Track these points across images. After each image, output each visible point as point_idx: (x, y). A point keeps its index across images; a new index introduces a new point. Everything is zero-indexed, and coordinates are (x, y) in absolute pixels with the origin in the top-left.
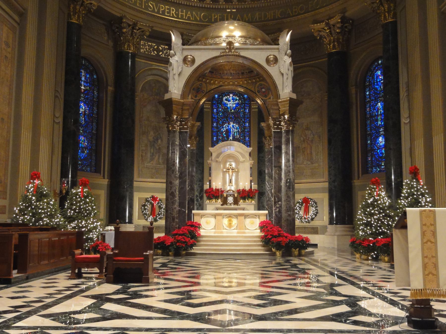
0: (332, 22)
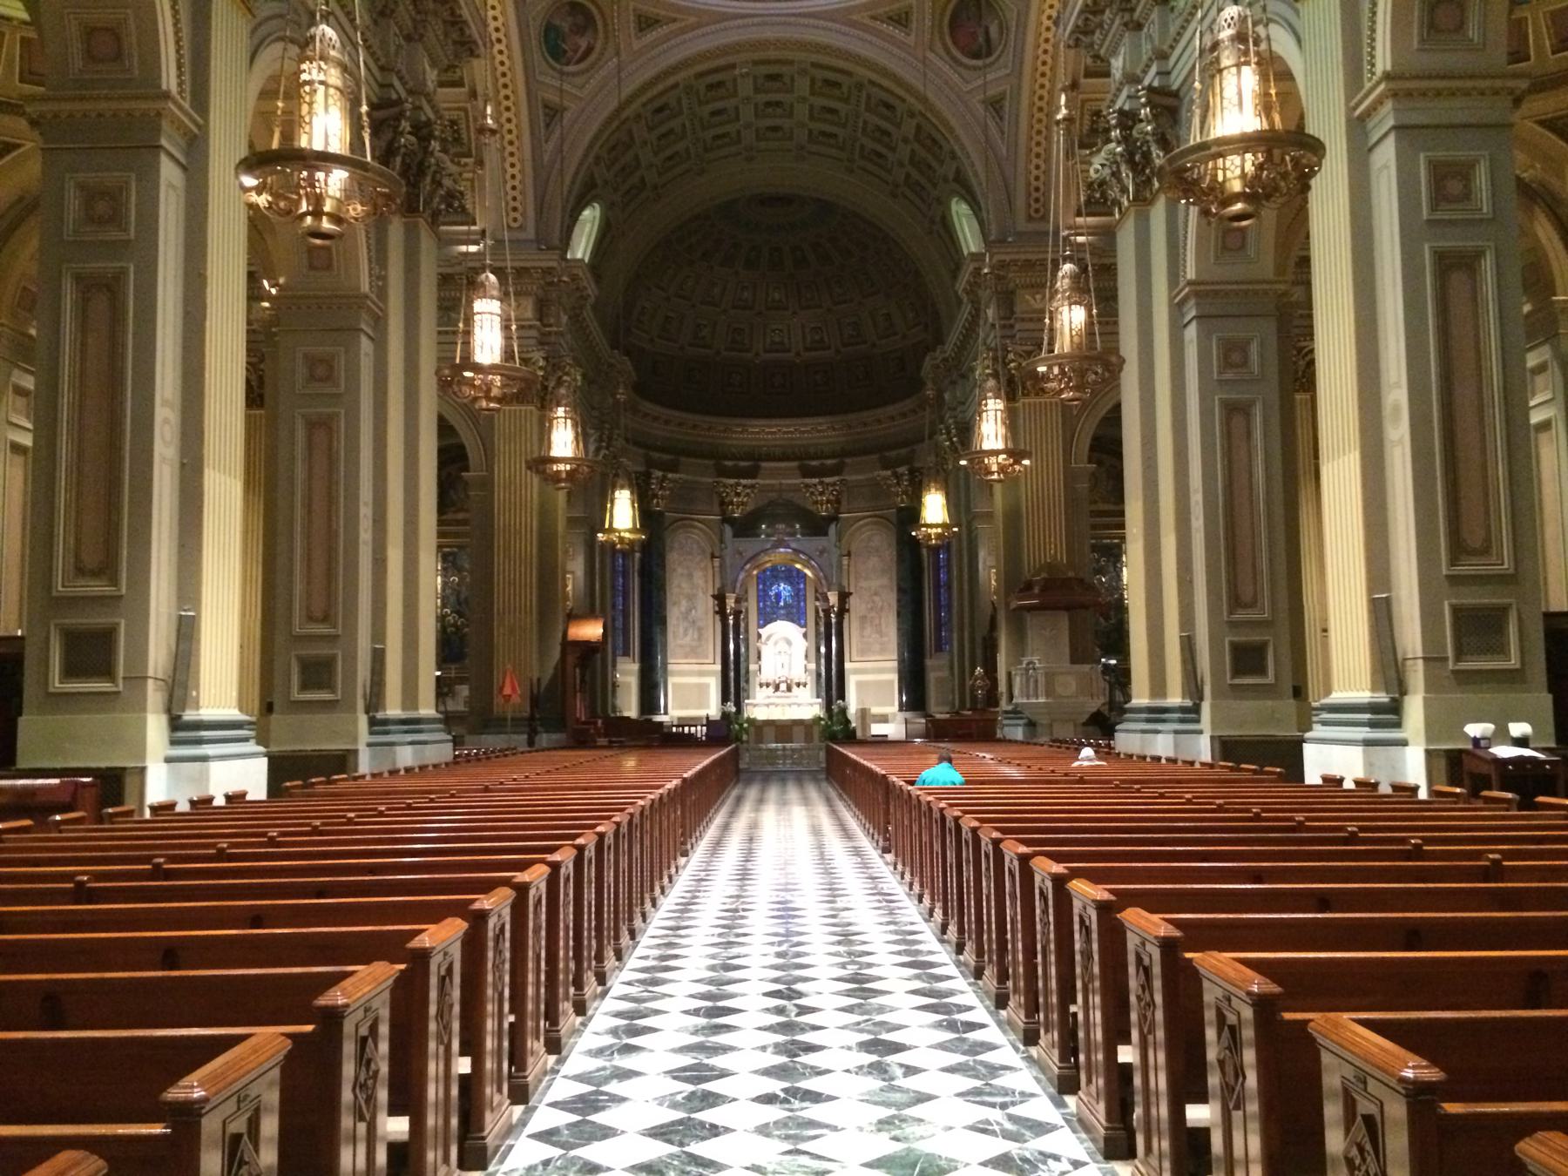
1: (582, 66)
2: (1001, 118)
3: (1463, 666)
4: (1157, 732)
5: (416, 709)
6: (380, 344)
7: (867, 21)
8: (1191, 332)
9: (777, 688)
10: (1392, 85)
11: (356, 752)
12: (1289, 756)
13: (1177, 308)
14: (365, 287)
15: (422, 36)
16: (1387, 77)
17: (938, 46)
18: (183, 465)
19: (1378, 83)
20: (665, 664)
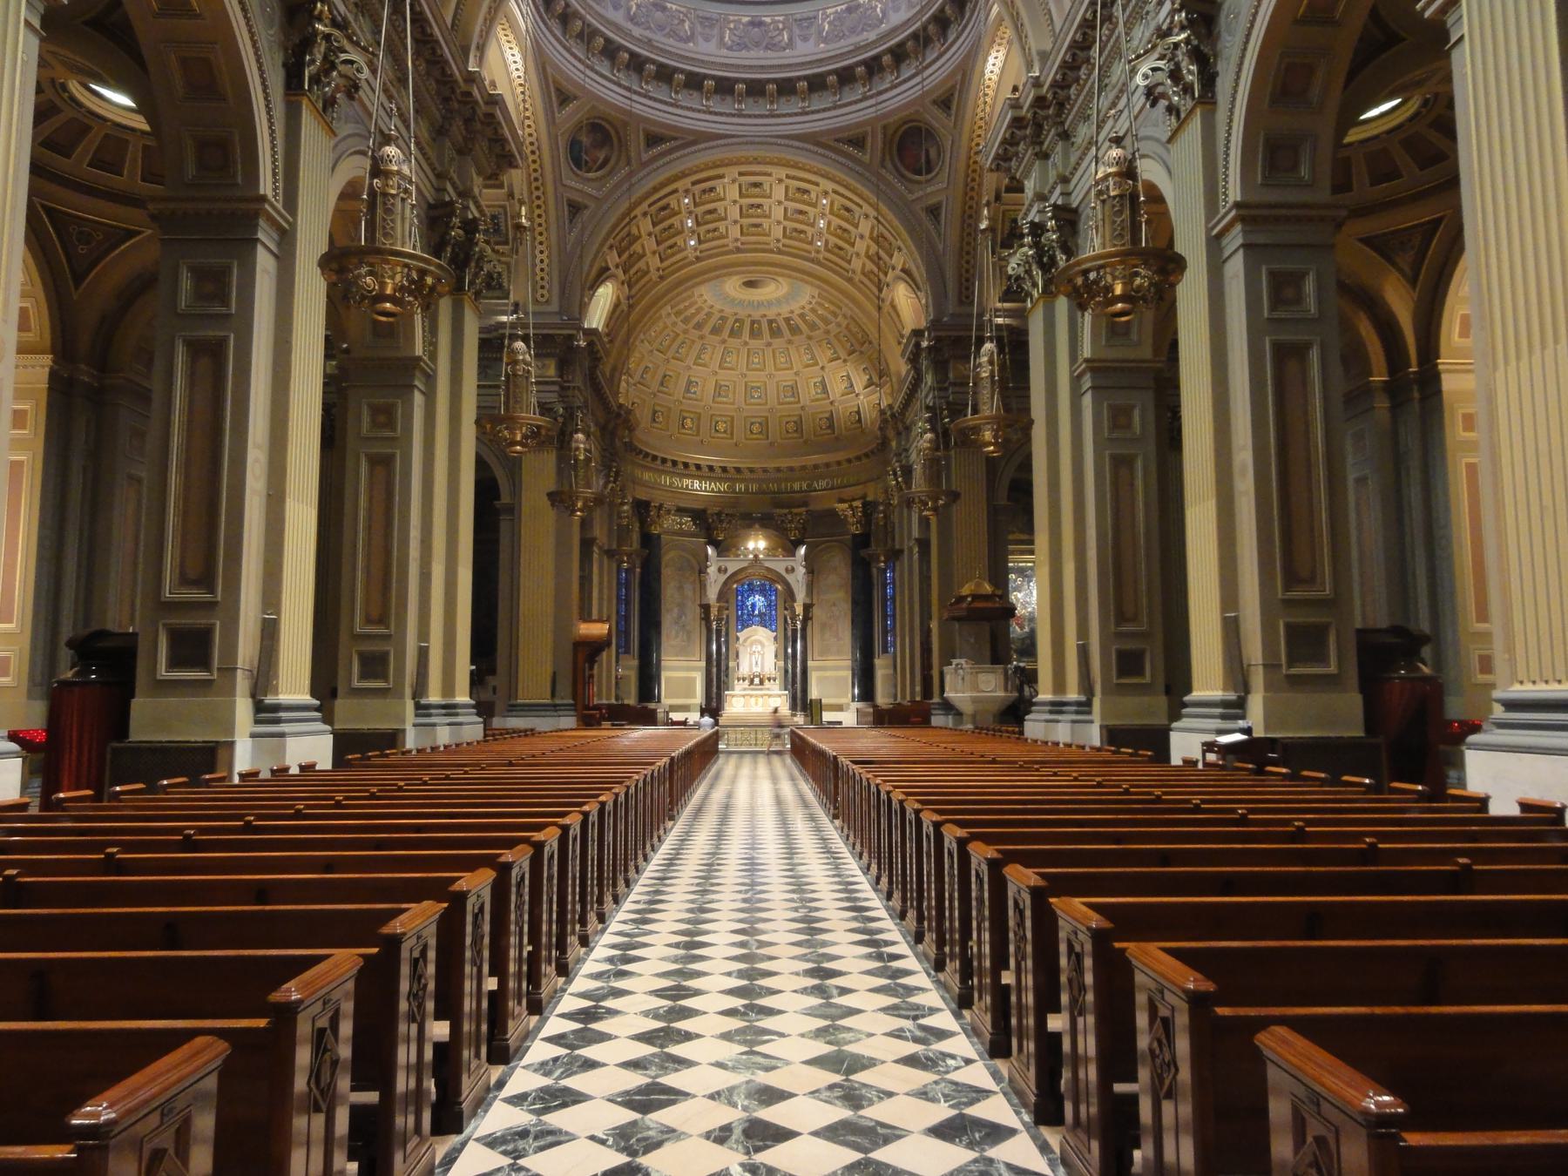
0: (855, 504)
1: (599, 174)
2: (939, 222)
3: (1294, 671)
4: (1058, 721)
5: (453, 696)
6: (430, 396)
7: (832, 144)
8: (1087, 400)
9: (752, 682)
10: (1242, 212)
11: (404, 731)
12: (1157, 742)
13: (1076, 381)
14: (419, 351)
15: (471, 150)
16: (1237, 205)
17: (889, 165)
18: (269, 495)
19: (1230, 210)
20: (659, 661)
